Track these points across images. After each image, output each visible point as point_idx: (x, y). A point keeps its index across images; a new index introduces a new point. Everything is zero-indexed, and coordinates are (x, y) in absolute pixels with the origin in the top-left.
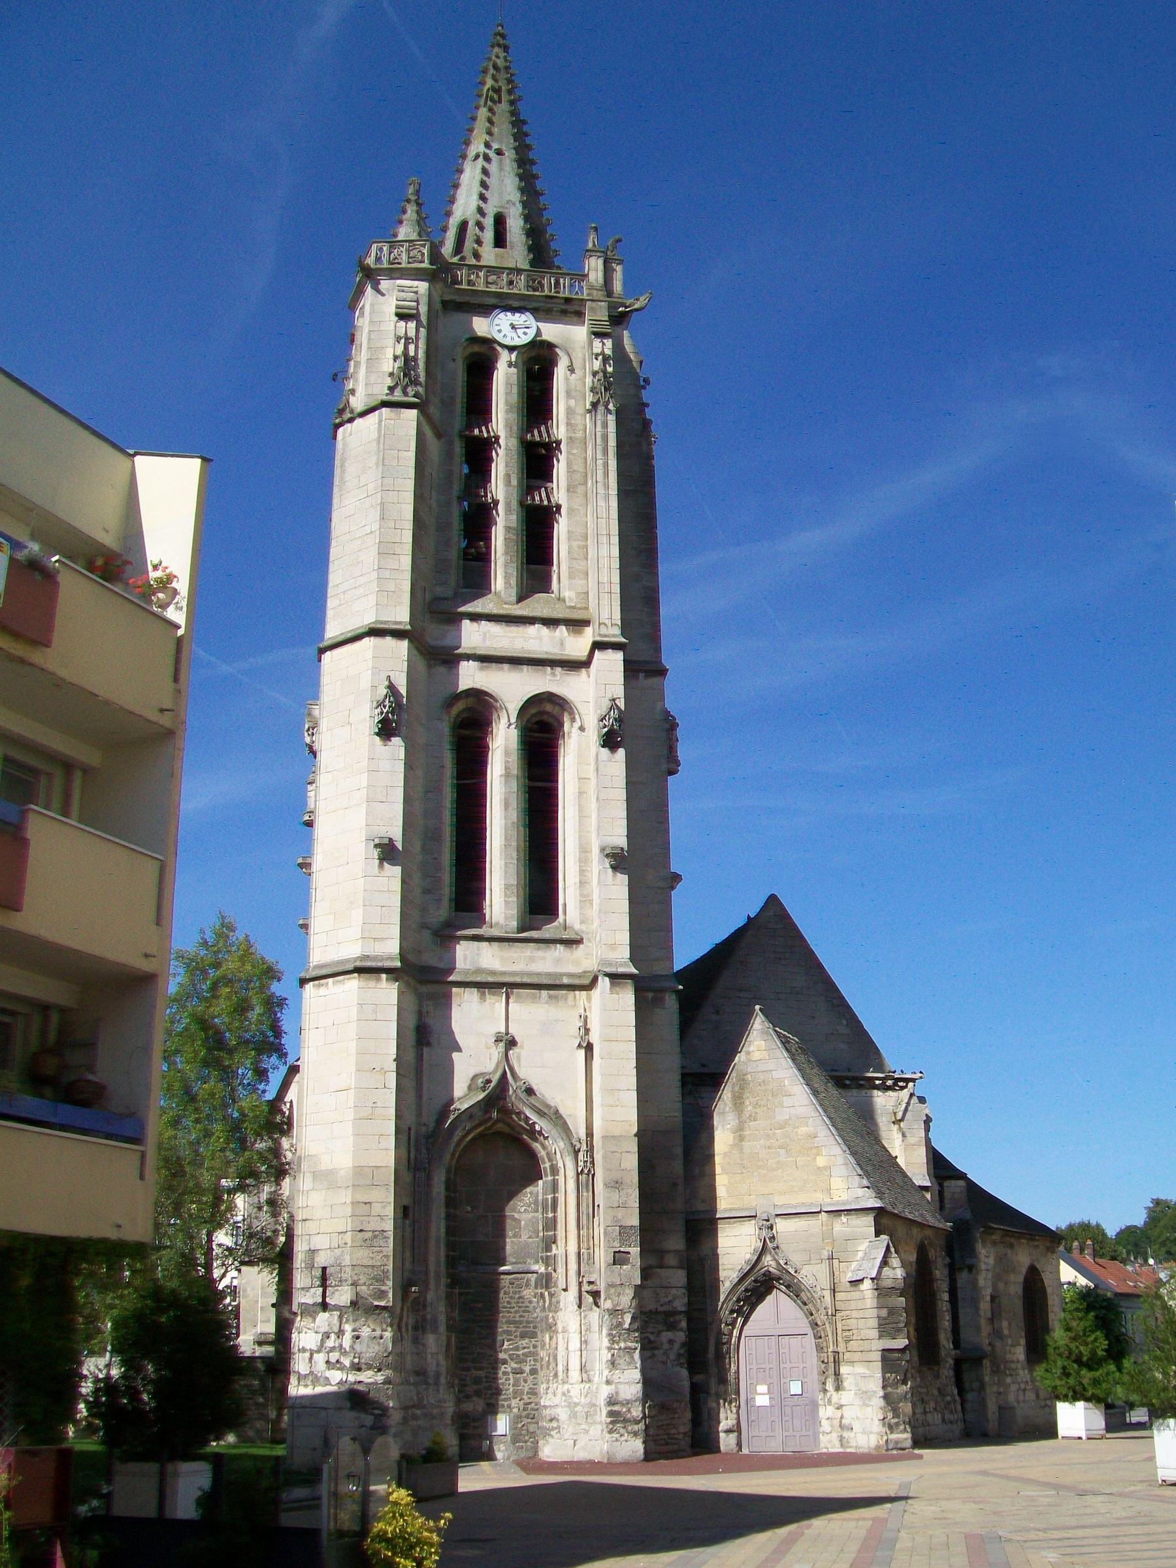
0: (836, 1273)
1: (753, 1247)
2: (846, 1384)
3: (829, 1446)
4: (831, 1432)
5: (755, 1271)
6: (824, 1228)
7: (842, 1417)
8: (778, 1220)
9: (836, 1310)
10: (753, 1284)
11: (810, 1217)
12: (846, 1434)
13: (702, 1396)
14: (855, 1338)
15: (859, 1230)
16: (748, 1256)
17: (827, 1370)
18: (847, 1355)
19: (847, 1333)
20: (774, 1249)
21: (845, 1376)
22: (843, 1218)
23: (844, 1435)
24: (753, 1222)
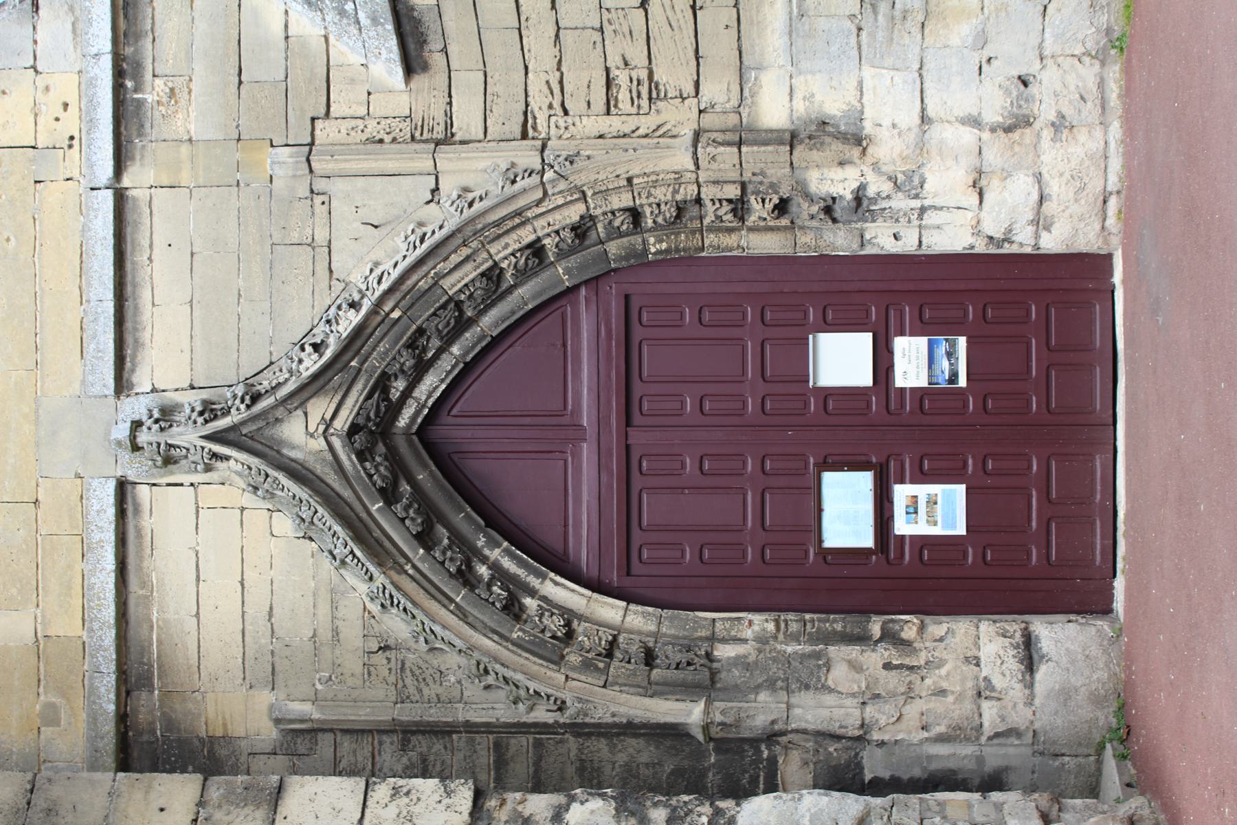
0: (373, 129)
1: (248, 500)
2: (834, 105)
3: (1095, 186)
4: (1039, 178)
5: (347, 494)
6: (185, 178)
7: (974, 122)
8: (142, 380)
9: (524, 136)
10: (399, 508)
11: (140, 237)
12: (1046, 113)
13: (874, 765)
14: (638, 55)
15: (201, 26)
16: (285, 524)
17: (774, 187)
18: (717, 90)
19: (624, 96)
20: (256, 398)
21: (800, 107)
22: (149, 97)
23: (1052, 116)
24: (143, 492)
